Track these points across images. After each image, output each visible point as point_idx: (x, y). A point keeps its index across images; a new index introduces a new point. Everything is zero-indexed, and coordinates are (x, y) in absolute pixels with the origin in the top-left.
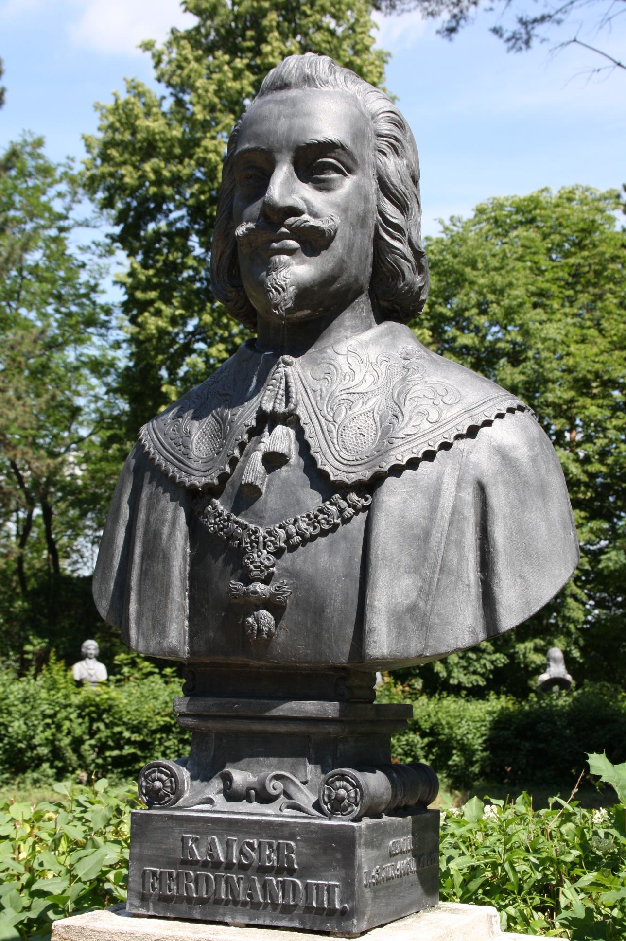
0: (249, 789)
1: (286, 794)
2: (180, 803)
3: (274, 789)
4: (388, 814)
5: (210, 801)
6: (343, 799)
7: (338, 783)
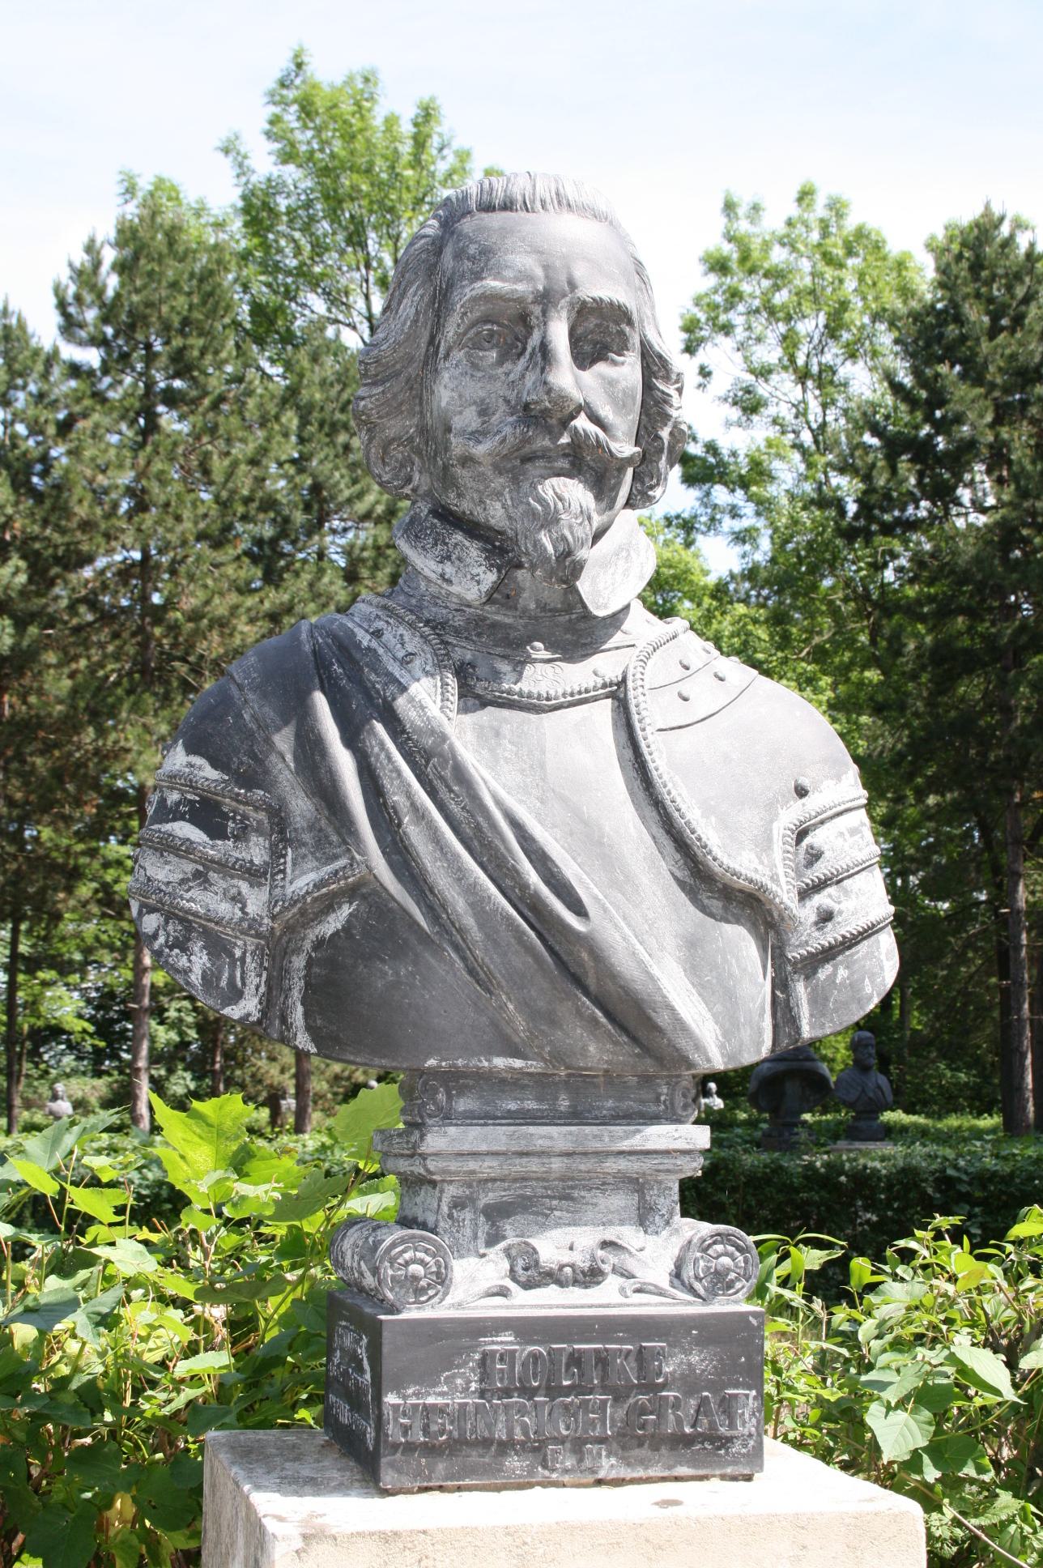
0: (562, 1267)
5: (503, 1292)
6: (728, 1270)
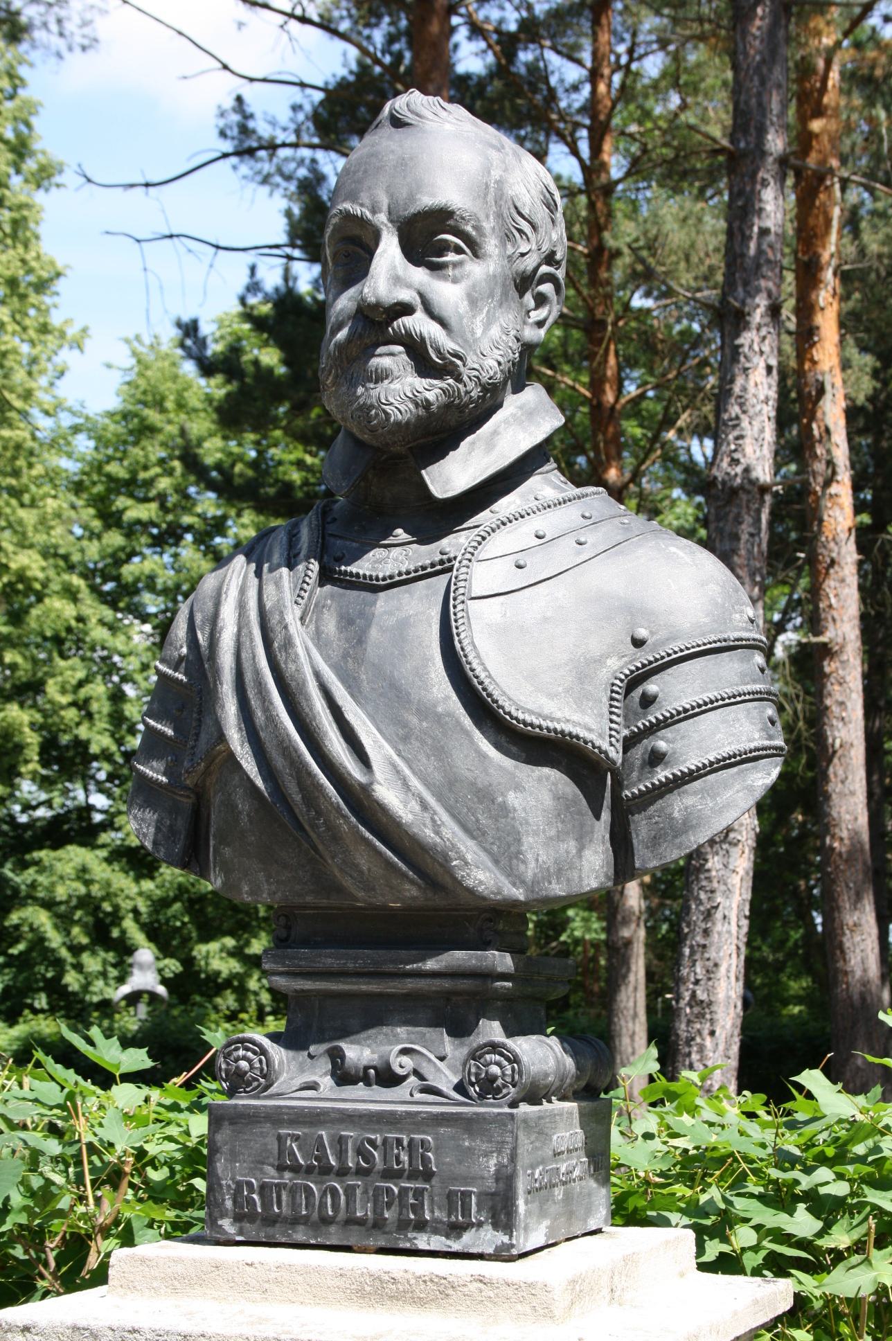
0: (366, 1068)
1: (416, 1073)
2: (272, 1090)
3: (401, 1067)
4: (559, 1100)
5: (313, 1086)
6: (495, 1078)
7: (488, 1057)
